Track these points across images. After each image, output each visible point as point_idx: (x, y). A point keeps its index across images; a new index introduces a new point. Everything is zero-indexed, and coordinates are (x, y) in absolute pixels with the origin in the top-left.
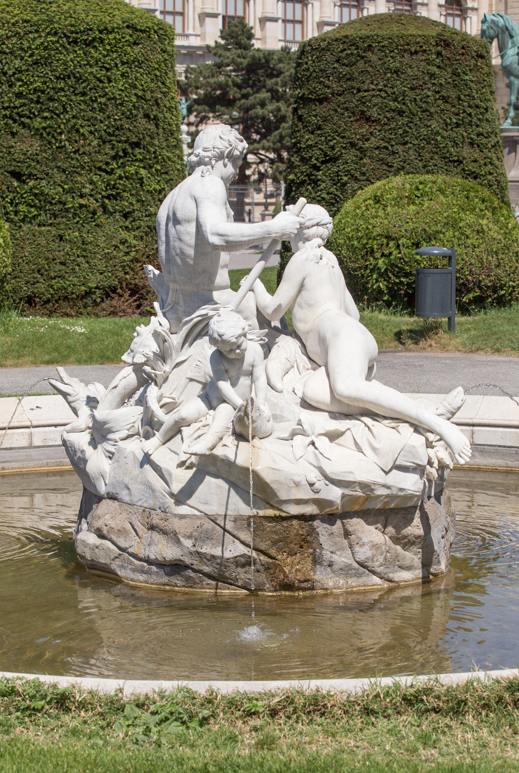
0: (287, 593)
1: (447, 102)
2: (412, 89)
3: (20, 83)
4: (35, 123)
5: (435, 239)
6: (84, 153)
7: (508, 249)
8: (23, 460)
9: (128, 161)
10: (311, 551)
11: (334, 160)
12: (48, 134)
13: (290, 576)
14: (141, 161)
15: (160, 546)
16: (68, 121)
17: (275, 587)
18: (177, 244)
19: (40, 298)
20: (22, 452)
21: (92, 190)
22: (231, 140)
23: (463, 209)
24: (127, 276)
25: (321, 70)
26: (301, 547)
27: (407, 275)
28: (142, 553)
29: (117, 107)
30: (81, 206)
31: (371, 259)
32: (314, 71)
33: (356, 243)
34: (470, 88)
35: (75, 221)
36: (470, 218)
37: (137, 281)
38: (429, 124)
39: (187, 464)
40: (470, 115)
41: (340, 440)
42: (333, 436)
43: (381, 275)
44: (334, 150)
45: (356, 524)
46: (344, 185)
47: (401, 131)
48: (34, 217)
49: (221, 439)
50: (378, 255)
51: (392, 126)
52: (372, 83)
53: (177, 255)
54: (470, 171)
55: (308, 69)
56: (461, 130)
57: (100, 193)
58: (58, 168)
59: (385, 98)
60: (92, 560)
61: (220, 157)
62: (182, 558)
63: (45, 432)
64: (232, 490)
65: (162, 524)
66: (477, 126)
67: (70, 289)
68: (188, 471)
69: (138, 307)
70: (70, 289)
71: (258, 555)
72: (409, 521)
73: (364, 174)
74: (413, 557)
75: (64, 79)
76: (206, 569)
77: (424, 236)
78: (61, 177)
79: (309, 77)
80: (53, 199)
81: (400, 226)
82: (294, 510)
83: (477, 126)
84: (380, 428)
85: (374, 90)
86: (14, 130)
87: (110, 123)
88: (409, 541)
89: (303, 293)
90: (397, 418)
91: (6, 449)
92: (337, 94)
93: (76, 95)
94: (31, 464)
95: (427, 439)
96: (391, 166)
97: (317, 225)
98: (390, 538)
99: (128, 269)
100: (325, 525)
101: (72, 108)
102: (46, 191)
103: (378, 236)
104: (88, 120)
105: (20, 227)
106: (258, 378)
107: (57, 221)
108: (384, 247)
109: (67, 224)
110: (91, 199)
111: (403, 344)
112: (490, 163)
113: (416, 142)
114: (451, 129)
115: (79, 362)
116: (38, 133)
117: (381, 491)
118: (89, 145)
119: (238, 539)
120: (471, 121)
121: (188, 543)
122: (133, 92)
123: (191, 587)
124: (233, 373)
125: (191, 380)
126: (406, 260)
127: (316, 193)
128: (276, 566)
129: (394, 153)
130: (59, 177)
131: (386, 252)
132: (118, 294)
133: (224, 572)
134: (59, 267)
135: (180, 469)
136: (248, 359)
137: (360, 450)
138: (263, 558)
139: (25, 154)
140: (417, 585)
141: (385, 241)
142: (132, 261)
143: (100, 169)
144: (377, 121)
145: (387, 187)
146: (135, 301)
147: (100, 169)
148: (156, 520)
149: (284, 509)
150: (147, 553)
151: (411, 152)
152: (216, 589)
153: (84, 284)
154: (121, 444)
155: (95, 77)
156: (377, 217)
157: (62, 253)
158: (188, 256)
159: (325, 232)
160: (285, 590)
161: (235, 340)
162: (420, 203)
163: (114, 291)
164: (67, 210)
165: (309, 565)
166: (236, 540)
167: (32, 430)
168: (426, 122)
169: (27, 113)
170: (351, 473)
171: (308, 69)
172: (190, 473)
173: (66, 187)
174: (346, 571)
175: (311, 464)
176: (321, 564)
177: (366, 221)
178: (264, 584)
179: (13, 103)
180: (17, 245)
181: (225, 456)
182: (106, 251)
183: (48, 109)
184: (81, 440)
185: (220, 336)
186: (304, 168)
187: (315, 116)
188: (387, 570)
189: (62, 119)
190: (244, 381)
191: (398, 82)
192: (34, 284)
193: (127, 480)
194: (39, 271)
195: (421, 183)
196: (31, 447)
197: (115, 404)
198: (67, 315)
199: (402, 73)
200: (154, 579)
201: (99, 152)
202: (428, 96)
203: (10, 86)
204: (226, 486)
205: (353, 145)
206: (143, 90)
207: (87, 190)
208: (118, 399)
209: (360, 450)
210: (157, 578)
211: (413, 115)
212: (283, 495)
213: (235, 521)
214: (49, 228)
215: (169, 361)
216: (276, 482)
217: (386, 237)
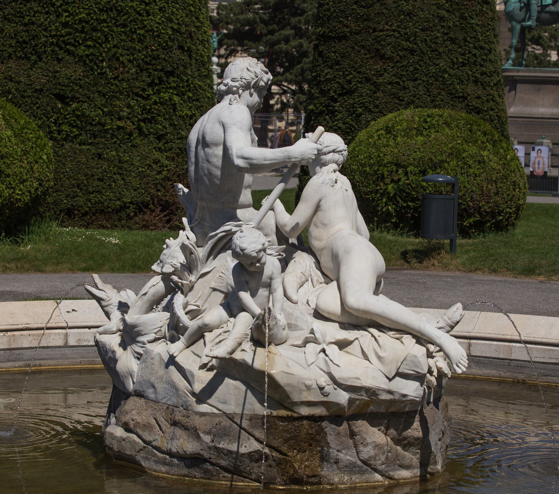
0: (296, 487)
1: (454, 43)
2: (423, 30)
3: (67, 14)
4: (79, 51)
5: (440, 167)
6: (123, 80)
7: (506, 179)
8: (58, 359)
9: (163, 88)
10: (319, 449)
11: (350, 93)
12: (91, 61)
13: (299, 471)
14: (175, 88)
15: (181, 440)
16: (109, 49)
17: (285, 481)
18: (206, 165)
19: (79, 211)
20: (58, 351)
21: (129, 114)
22: (256, 71)
23: (466, 141)
24: (159, 193)
25: (341, 11)
26: (310, 445)
27: (413, 200)
28: (165, 446)
29: (154, 39)
30: (119, 128)
31: (382, 184)
32: (335, 11)
33: (368, 169)
34: (476, 31)
35: (113, 141)
36: (472, 149)
37: (167, 197)
38: (438, 62)
39: (208, 367)
40: (475, 55)
41: (349, 349)
42: (342, 345)
43: (390, 199)
44: (351, 84)
45: (362, 425)
46: (359, 115)
47: (411, 69)
48: (76, 137)
49: (240, 344)
50: (388, 181)
51: (404, 64)
52: (387, 24)
53: (205, 175)
54: (474, 106)
55: (329, 10)
56: (466, 69)
57: (136, 117)
58: (99, 92)
59: (398, 38)
60: (119, 452)
61: (247, 87)
62: (201, 452)
63: (80, 333)
64: (249, 391)
65: (184, 420)
66: (481, 66)
67: (106, 204)
68: (209, 372)
69: (168, 221)
70: (106, 204)
71: (271, 451)
72: (409, 425)
73: (377, 107)
74: (412, 457)
75: (106, 11)
76: (223, 463)
77: (430, 165)
78: (101, 101)
79: (330, 16)
80: (94, 120)
81: (408, 155)
82: (305, 411)
83: (481, 66)
84: (386, 339)
85: (388, 30)
86: (60, 57)
87: (147, 52)
88: (409, 442)
89: (319, 214)
90: (401, 330)
91: (44, 347)
92: (355, 33)
93: (117, 26)
94: (66, 362)
95: (428, 350)
96: (402, 100)
97: (334, 151)
98: (392, 439)
99: (159, 187)
100: (333, 426)
101: (113, 38)
102: (88, 113)
103: (388, 163)
104: (128, 50)
105: (63, 145)
106: (275, 290)
107: (96, 141)
108: (394, 174)
109: (105, 144)
110: (128, 122)
111: (409, 263)
112: (492, 99)
113: (425, 79)
114: (458, 68)
115: (112, 270)
116: (81, 60)
117: (384, 396)
118: (128, 72)
119: (253, 436)
120: (476, 61)
121: (207, 439)
122: (170, 25)
123: (209, 479)
124: (253, 284)
125: (214, 290)
126: (413, 186)
127: (333, 122)
128: (287, 462)
129: (405, 88)
130: (99, 101)
131: (396, 178)
132: (150, 209)
133: (239, 466)
134: (96, 183)
135: (201, 371)
136: (267, 271)
137: (365, 357)
138: (274, 454)
139: (69, 79)
140: (415, 482)
141: (395, 168)
142: (163, 179)
143: (137, 94)
144: (391, 59)
145: (397, 119)
146: (165, 216)
147: (137, 94)
148: (178, 417)
149: (296, 410)
150: (169, 446)
151: (420, 88)
152: (232, 481)
153: (119, 199)
154: (148, 346)
155: (135, 10)
156: (388, 146)
157: (100, 170)
158: (215, 177)
159: (340, 158)
160: (294, 484)
161: (256, 255)
162: (427, 135)
163: (147, 206)
164: (106, 131)
165: (317, 462)
166: (251, 437)
167: (68, 331)
168: (435, 61)
169: (72, 41)
170: (358, 379)
171: (329, 10)
172: (211, 375)
173: (105, 110)
174: (351, 468)
175: (321, 369)
176: (328, 461)
177: (378, 149)
178: (275, 478)
179: (60, 31)
180: (60, 161)
181: (244, 360)
182: (140, 170)
183: (91, 39)
184: (113, 341)
185: (242, 250)
186: (322, 100)
187: (335, 52)
188: (387, 468)
189: (104, 48)
190: (263, 292)
191: (410, 24)
192: (74, 197)
193: (153, 379)
194: (78, 186)
195: (429, 116)
196: (66, 346)
197: (144, 309)
198: (104, 227)
199: (414, 16)
200: (175, 470)
201: (137, 79)
202: (437, 37)
203: (58, 16)
204: (243, 388)
205: (368, 80)
206: (179, 24)
207: (125, 114)
208: (146, 305)
209: (365, 357)
210: (179, 470)
211: (423, 53)
212: (296, 398)
213: (250, 420)
214: (89, 147)
215: (195, 272)
216: (289, 385)
217: (396, 165)
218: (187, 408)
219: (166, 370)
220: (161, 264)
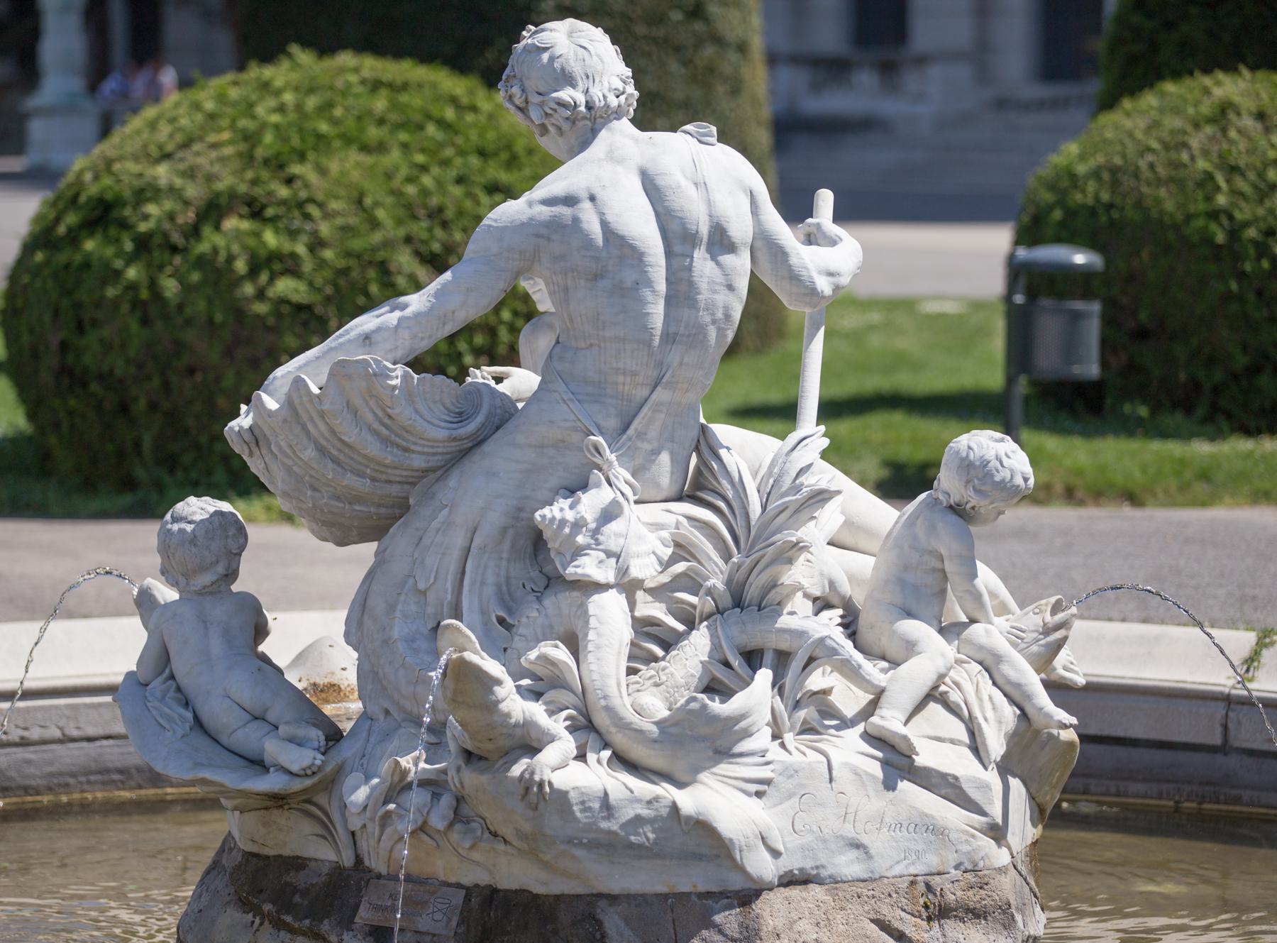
65: (973, 898)
193: (848, 831)
218: (976, 865)
220: (613, 560)
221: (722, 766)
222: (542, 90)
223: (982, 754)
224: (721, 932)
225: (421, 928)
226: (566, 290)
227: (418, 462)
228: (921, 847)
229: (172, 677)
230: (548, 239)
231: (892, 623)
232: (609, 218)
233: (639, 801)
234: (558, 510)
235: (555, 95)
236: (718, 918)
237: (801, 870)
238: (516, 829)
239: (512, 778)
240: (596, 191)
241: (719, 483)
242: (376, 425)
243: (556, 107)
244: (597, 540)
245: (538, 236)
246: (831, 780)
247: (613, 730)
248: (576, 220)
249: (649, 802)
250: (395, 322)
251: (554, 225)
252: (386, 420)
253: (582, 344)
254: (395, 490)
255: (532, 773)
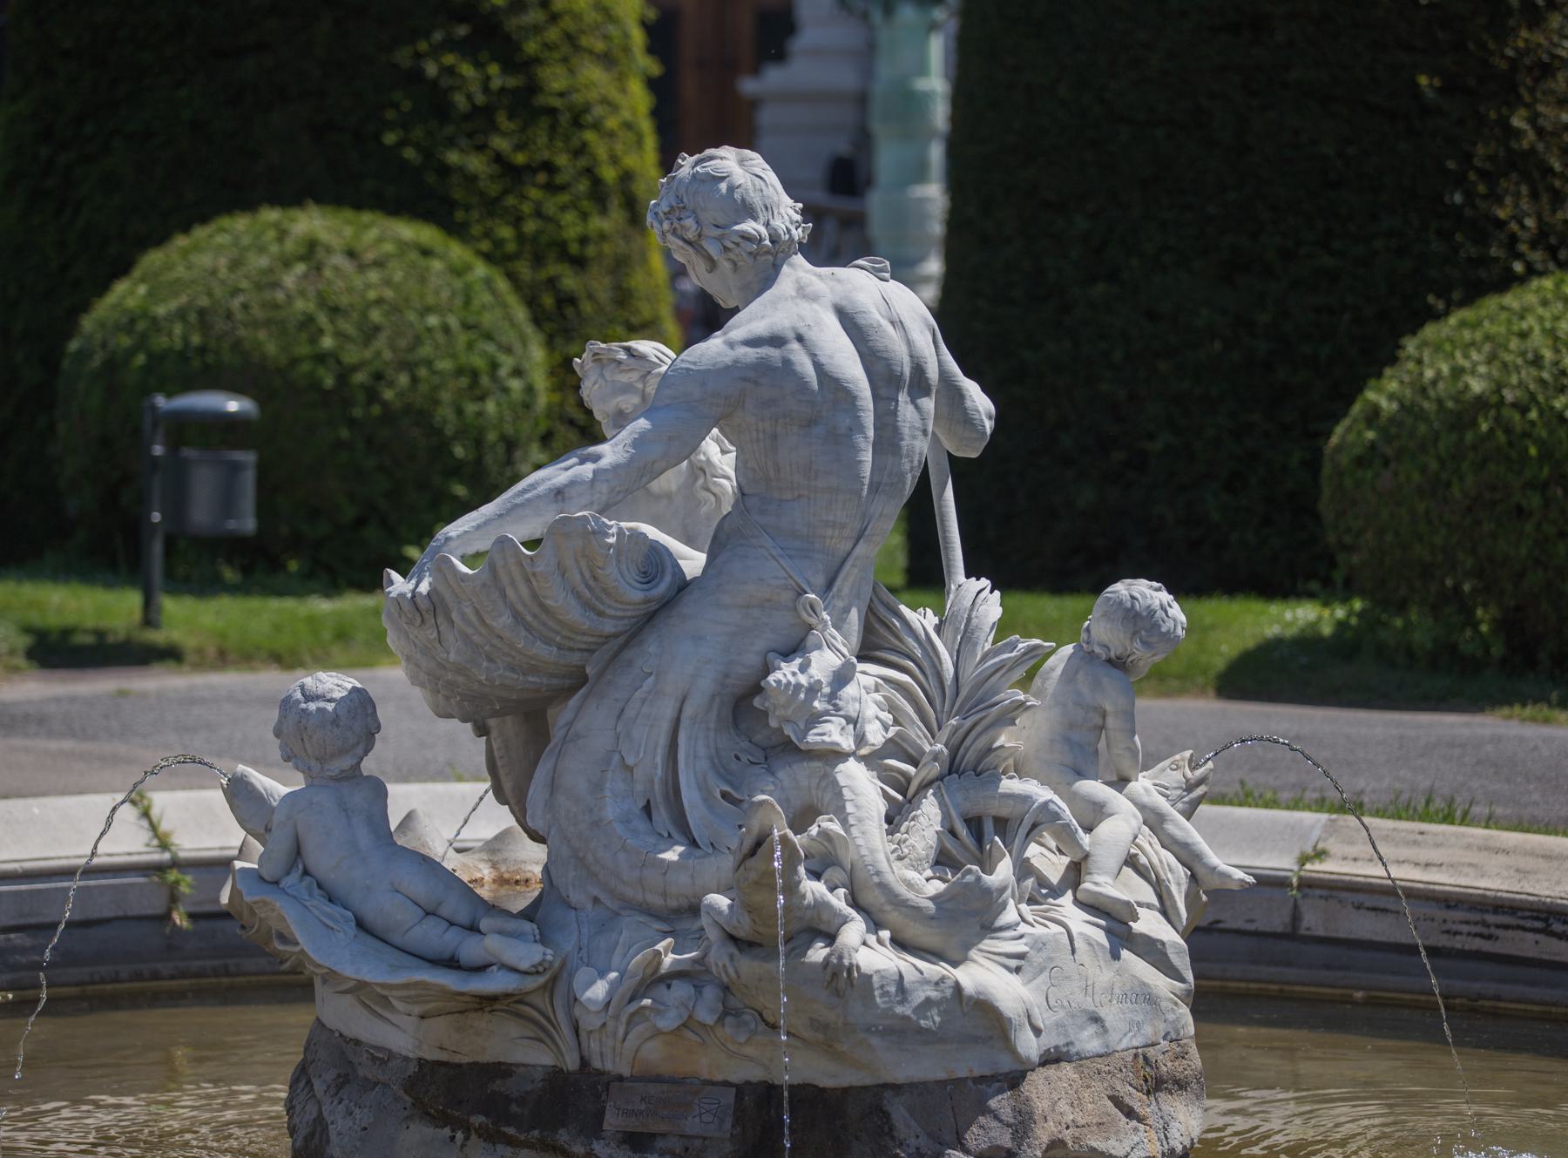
193: (1089, 1004)
219: (1116, 964)
221: (986, 941)
222: (721, 222)
223: (1173, 918)
224: (996, 1118)
225: (689, 1132)
226: (775, 437)
227: (609, 627)
228: (1140, 1018)
229: (306, 872)
230: (756, 383)
231: (1070, 784)
232: (823, 360)
233: (926, 982)
234: (786, 673)
235: (736, 228)
236: (993, 1103)
237: (1056, 1047)
238: (812, 1019)
239: (813, 965)
240: (803, 330)
241: (901, 640)
242: (581, 588)
243: (739, 240)
244: (835, 705)
245: (745, 380)
246: (1073, 951)
247: (888, 908)
248: (787, 363)
249: (937, 984)
250: (590, 475)
251: (762, 367)
252: (591, 582)
253: (788, 496)
254: (575, 658)
255: (841, 958)
